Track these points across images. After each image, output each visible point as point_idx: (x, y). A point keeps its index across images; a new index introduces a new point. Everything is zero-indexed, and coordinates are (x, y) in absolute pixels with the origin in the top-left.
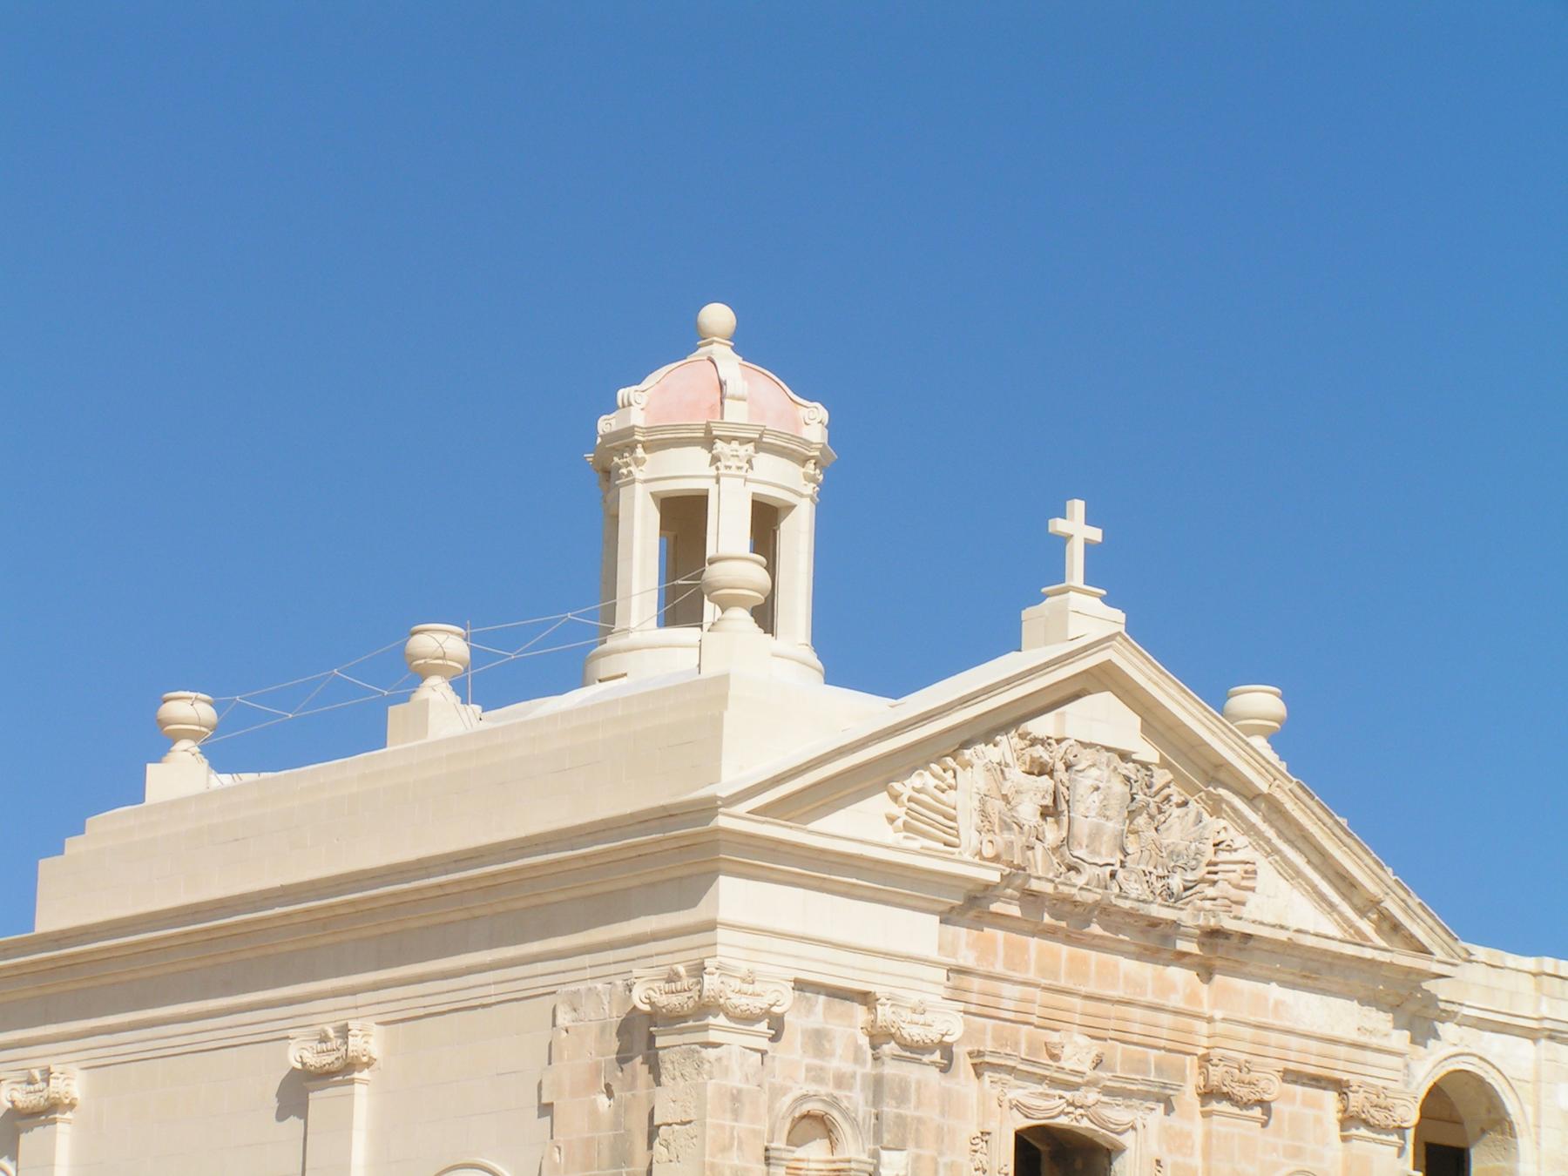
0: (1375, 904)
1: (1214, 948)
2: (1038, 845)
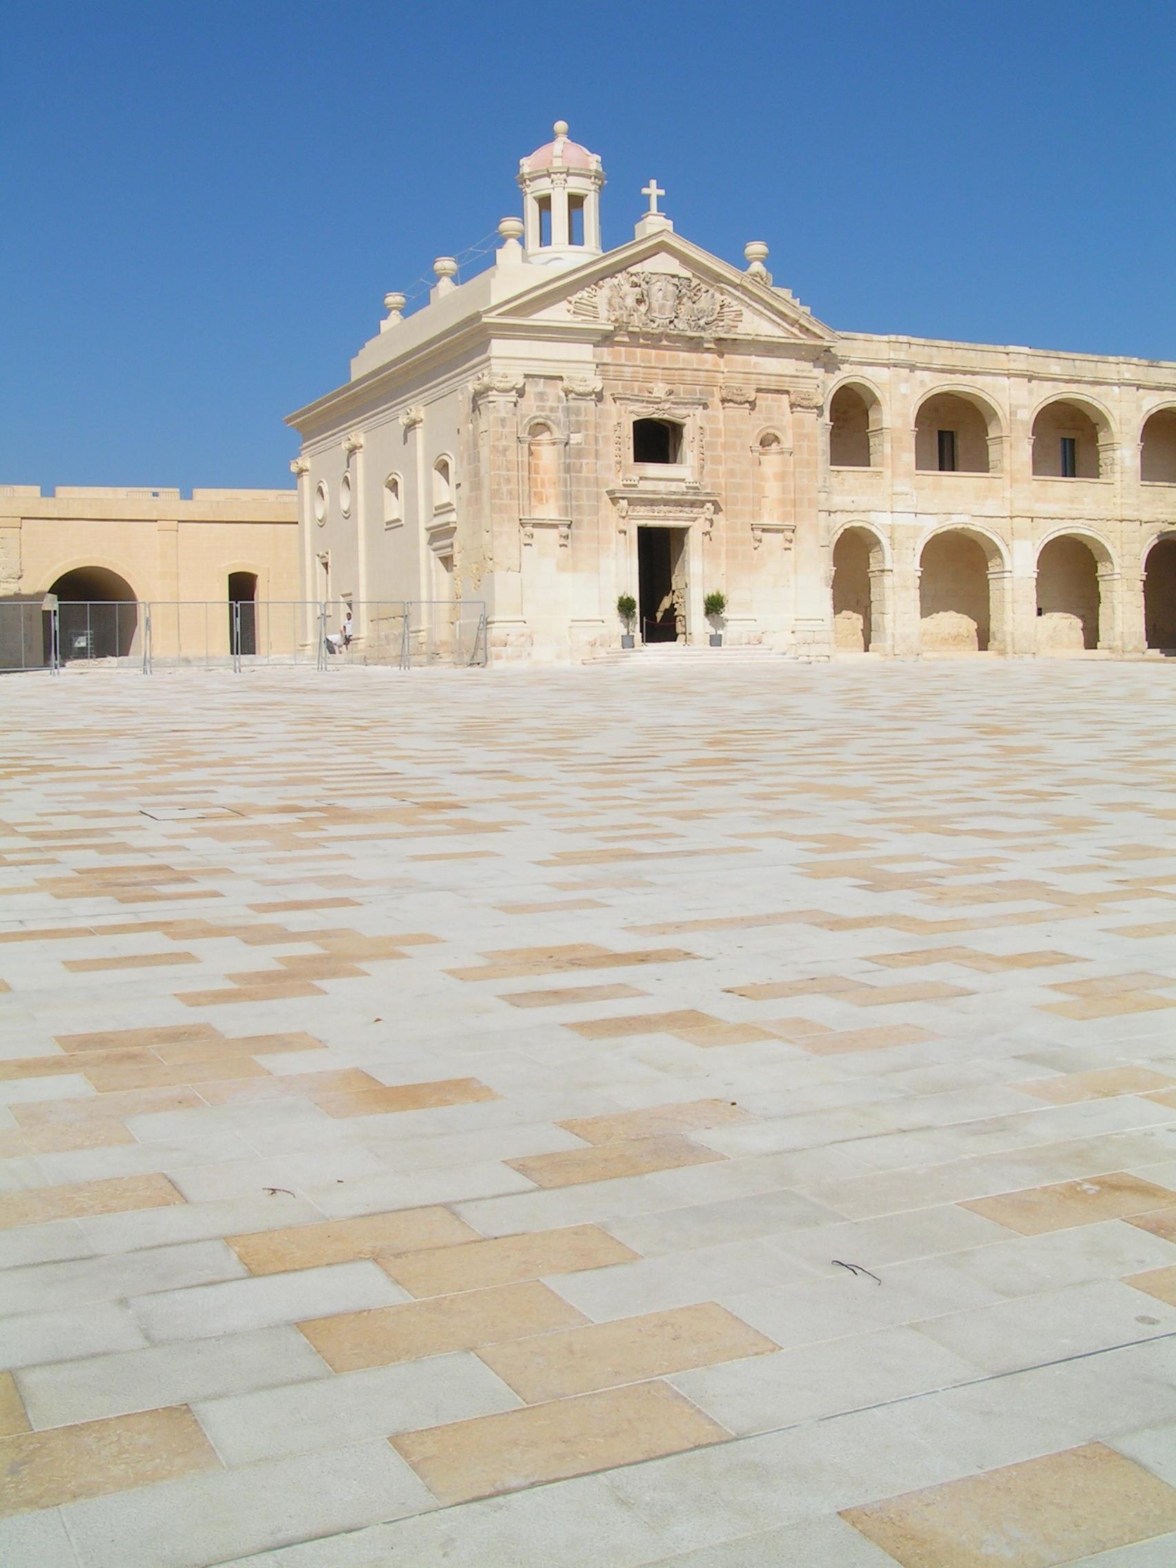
0: (797, 321)
2: (635, 314)
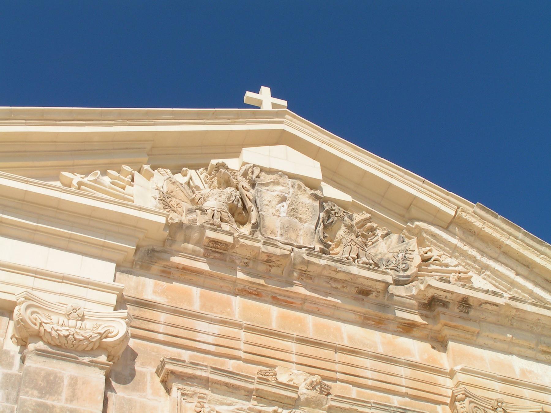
1: (435, 319)
